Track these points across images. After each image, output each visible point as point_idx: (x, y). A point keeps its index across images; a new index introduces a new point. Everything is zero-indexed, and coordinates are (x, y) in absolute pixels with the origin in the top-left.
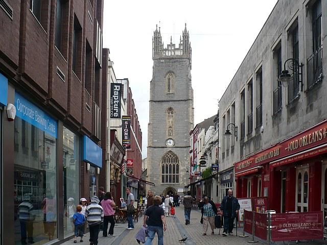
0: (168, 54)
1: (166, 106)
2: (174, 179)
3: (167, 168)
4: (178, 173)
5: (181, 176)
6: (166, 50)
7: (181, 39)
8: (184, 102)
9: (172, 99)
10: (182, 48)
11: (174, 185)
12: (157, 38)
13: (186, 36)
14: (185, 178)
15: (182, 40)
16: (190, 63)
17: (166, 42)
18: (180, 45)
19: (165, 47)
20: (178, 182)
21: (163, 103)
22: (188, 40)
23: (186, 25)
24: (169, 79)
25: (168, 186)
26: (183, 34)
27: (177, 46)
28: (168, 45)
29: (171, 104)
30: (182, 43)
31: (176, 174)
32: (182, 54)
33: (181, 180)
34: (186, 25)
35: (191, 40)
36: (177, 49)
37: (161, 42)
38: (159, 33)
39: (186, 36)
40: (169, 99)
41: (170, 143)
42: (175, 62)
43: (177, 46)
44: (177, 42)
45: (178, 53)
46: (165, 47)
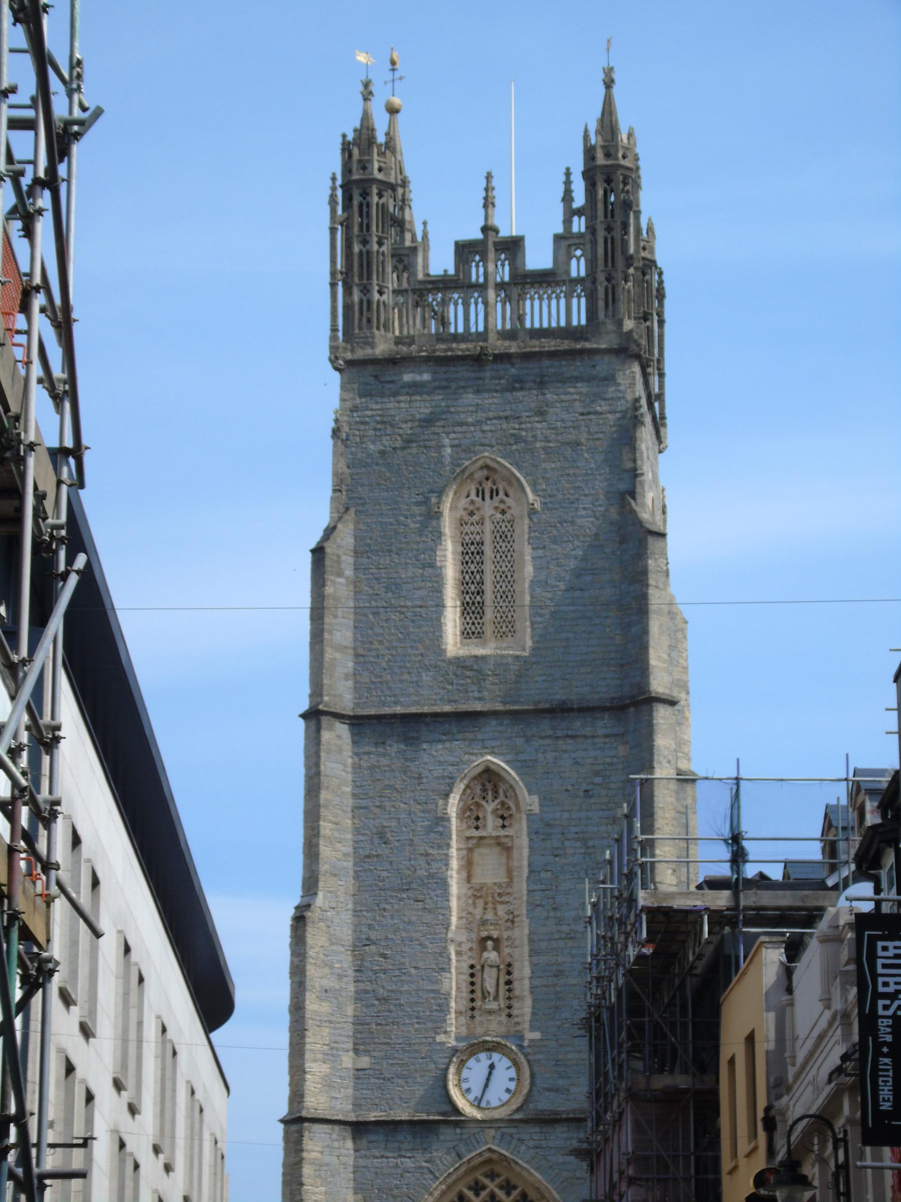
0: (465, 317)
6: (444, 284)
7: (568, 197)
8: (603, 725)
10: (578, 268)
13: (608, 179)
15: (579, 199)
16: (655, 398)
17: (441, 223)
18: (564, 242)
19: (440, 261)
22: (629, 206)
23: (609, 84)
26: (589, 153)
27: (539, 256)
28: (465, 251)
30: (579, 225)
32: (580, 318)
34: (609, 84)
35: (657, 204)
36: (544, 280)
37: (400, 224)
38: (390, 146)
39: (608, 179)
44: (537, 223)
45: (545, 312)
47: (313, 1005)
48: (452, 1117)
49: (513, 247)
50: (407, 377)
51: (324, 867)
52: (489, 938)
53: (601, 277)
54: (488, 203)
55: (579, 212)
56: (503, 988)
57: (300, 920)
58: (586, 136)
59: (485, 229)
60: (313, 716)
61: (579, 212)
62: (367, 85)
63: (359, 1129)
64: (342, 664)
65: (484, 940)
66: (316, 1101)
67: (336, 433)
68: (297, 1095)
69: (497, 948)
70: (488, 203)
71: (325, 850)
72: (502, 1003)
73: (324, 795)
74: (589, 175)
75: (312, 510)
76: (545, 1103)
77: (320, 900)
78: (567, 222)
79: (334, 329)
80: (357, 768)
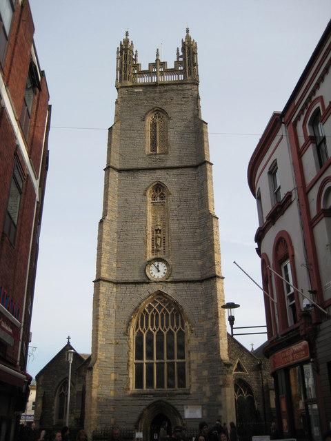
1: (147, 180)
2: (171, 376)
3: (150, 342)
4: (183, 357)
5: (194, 366)
7: (178, 53)
9: (162, 166)
11: (171, 395)
12: (126, 52)
13: (189, 51)
14: (205, 373)
17: (144, 62)
18: (177, 63)
20: (182, 385)
21: (140, 174)
24: (154, 125)
25: (156, 399)
26: (183, 43)
29: (160, 176)
31: (176, 360)
33: (194, 379)
39: (189, 51)
40: (154, 165)
41: (158, 272)
42: (166, 91)
43: (171, 66)
46: (145, 67)
47: (104, 246)
48: (147, 281)
49: (163, 64)
50: (136, 90)
51: (109, 208)
52: (158, 229)
53: (187, 68)
54: (157, 55)
55: (181, 57)
56: (162, 244)
57: (101, 222)
58: (182, 41)
59: (156, 60)
60: (108, 169)
61: (181, 57)
62: (127, 32)
63: (117, 283)
64: (115, 156)
65: (156, 230)
66: (104, 275)
67: (116, 103)
68: (99, 272)
69: (160, 233)
70: (157, 55)
71: (110, 204)
72: (162, 248)
73: (109, 189)
74: (183, 49)
75: (108, 117)
76: (176, 277)
77: (107, 217)
78: (178, 58)
79: (117, 79)
80: (120, 183)
